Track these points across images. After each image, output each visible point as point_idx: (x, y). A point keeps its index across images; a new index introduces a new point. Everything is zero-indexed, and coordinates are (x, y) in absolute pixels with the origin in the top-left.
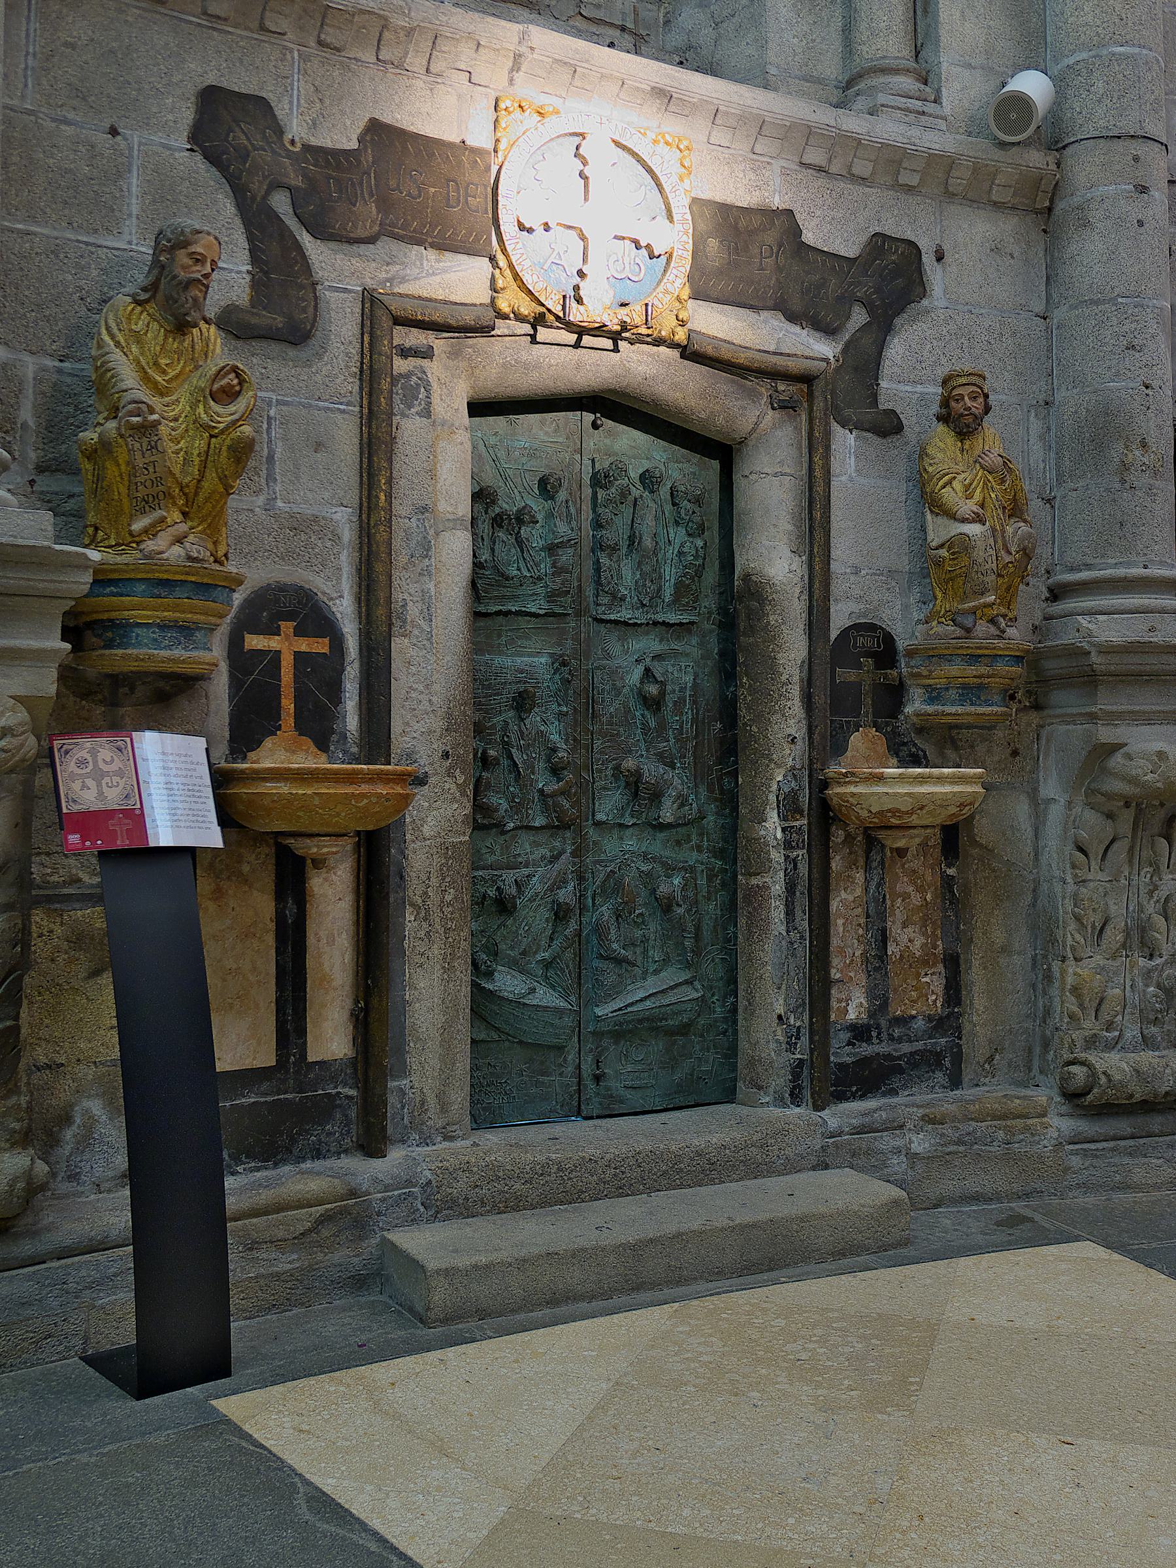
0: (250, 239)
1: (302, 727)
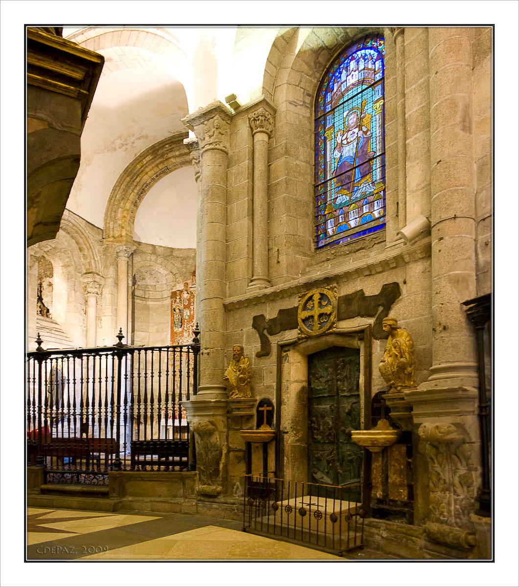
0: (261, 340)
1: (267, 423)
